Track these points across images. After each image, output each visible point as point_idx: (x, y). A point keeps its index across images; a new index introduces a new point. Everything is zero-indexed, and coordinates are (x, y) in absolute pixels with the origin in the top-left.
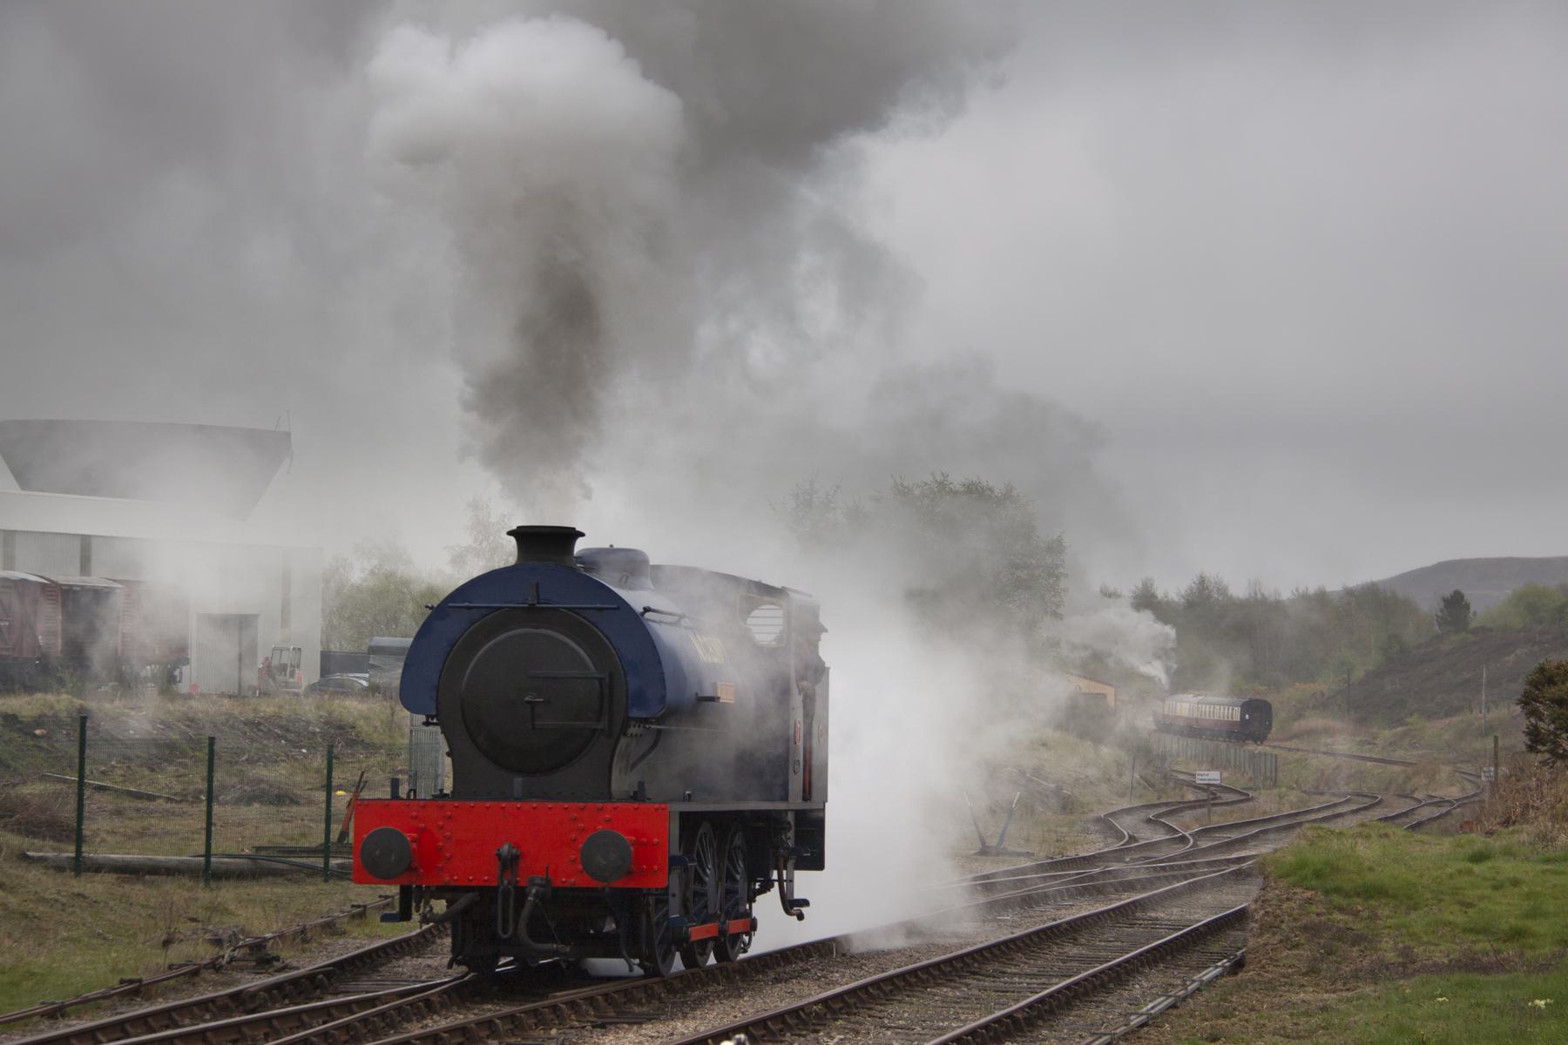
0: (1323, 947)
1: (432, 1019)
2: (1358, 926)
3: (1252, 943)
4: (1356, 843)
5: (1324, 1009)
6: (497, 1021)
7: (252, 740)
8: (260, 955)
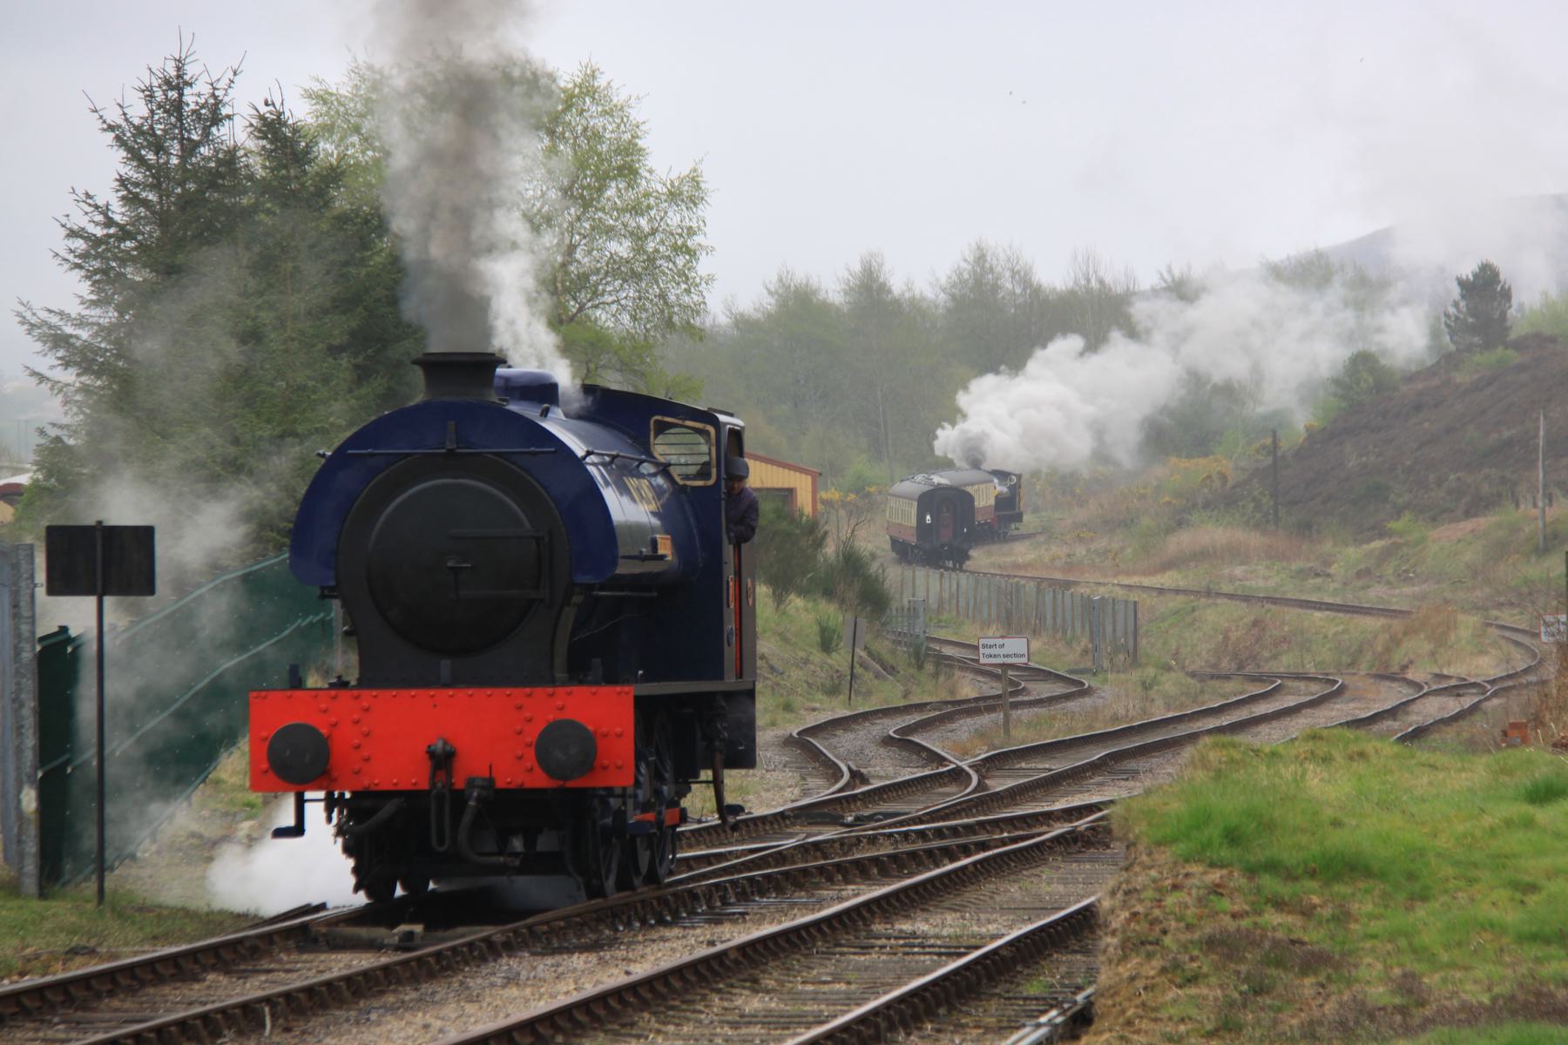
0: (1247, 980)
2: (1315, 937)
3: (1105, 977)
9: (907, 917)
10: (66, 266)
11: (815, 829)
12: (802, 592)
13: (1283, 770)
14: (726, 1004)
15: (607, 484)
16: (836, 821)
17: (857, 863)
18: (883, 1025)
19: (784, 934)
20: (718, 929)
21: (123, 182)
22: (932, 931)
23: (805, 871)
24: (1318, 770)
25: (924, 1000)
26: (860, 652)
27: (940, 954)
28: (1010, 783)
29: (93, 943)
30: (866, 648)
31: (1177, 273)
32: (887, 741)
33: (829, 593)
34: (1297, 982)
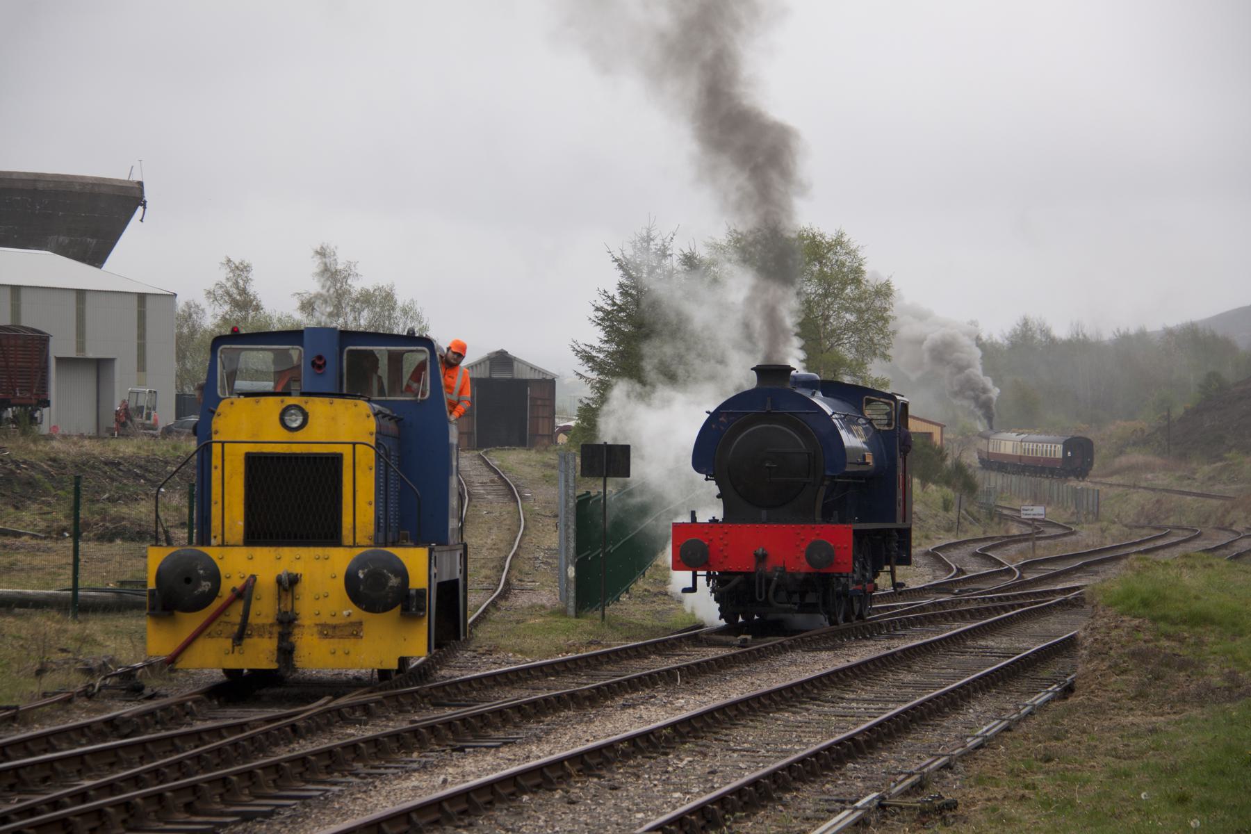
0: (1151, 672)
1: (298, 743)
2: (1185, 652)
3: (1080, 669)
4: (1181, 573)
5: (1153, 731)
6: (362, 745)
7: (112, 479)
8: (130, 684)
9: (984, 638)
10: (595, 324)
11: (940, 595)
12: (935, 483)
13: (1171, 572)
14: (895, 677)
15: (842, 428)
16: (950, 592)
17: (959, 612)
18: (971, 690)
19: (924, 645)
20: (892, 642)
21: (621, 285)
22: (995, 646)
23: (934, 615)
24: (1188, 572)
25: (991, 678)
26: (963, 512)
27: (999, 657)
28: (1035, 576)
29: (600, 639)
30: (965, 510)
31: (1122, 332)
32: (975, 554)
33: (948, 483)
34: (1176, 674)
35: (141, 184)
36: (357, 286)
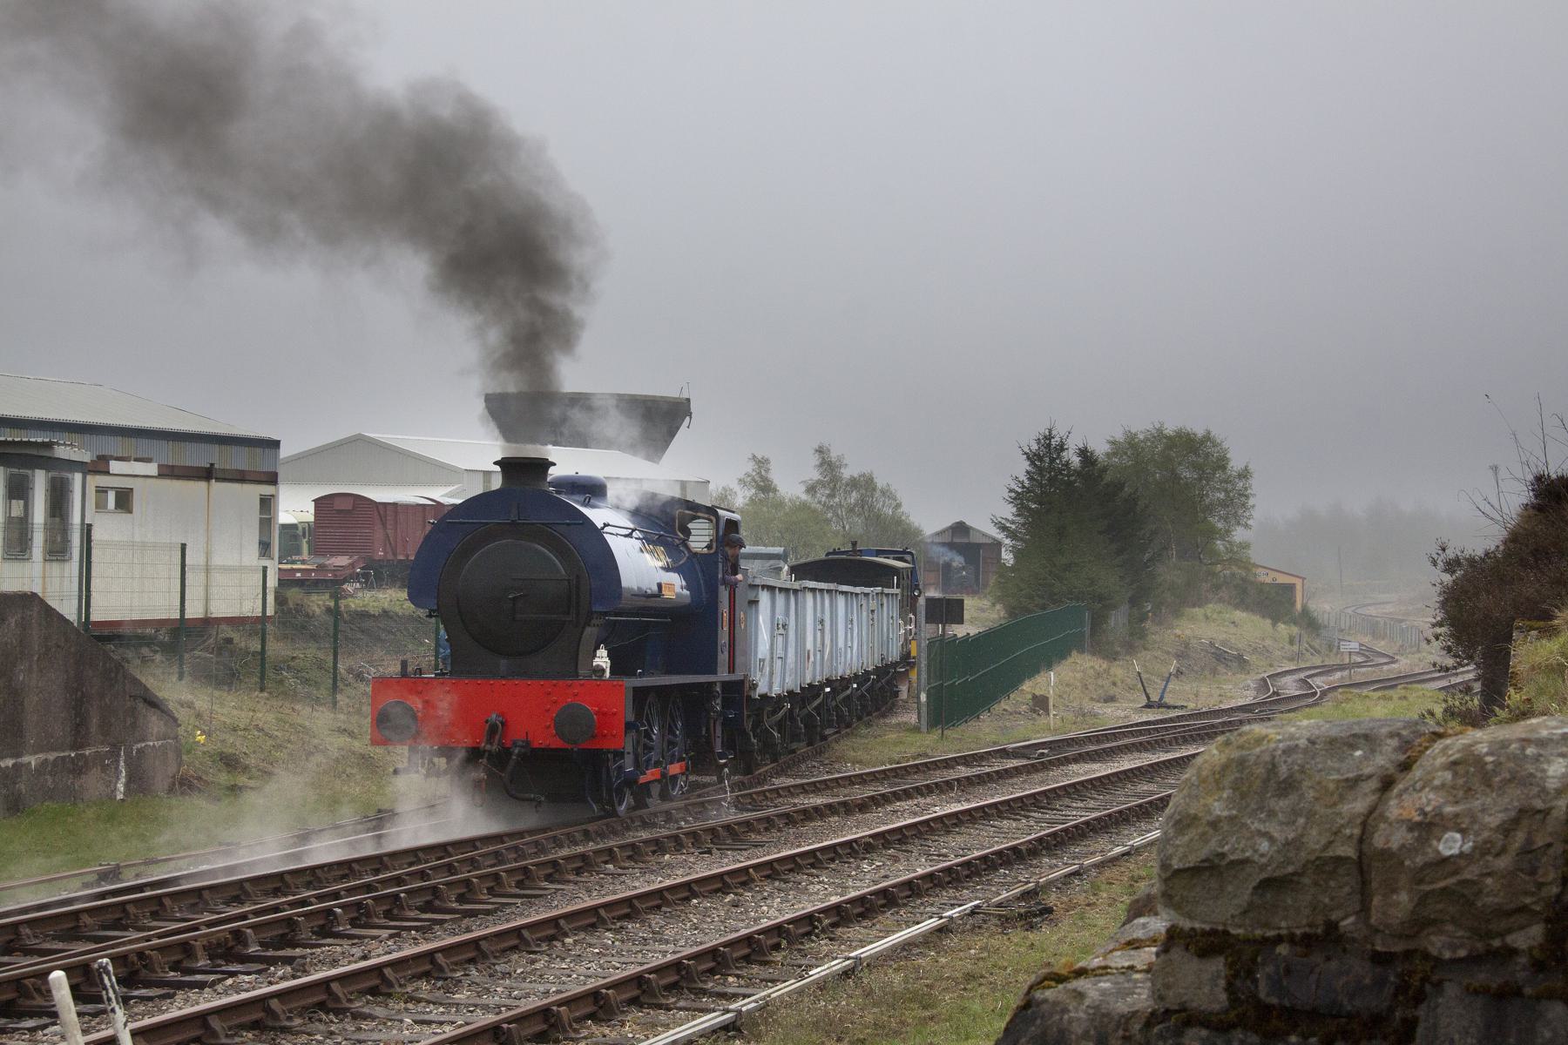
12: (1284, 623)
21: (1028, 472)
35: (688, 400)
36: (847, 473)
